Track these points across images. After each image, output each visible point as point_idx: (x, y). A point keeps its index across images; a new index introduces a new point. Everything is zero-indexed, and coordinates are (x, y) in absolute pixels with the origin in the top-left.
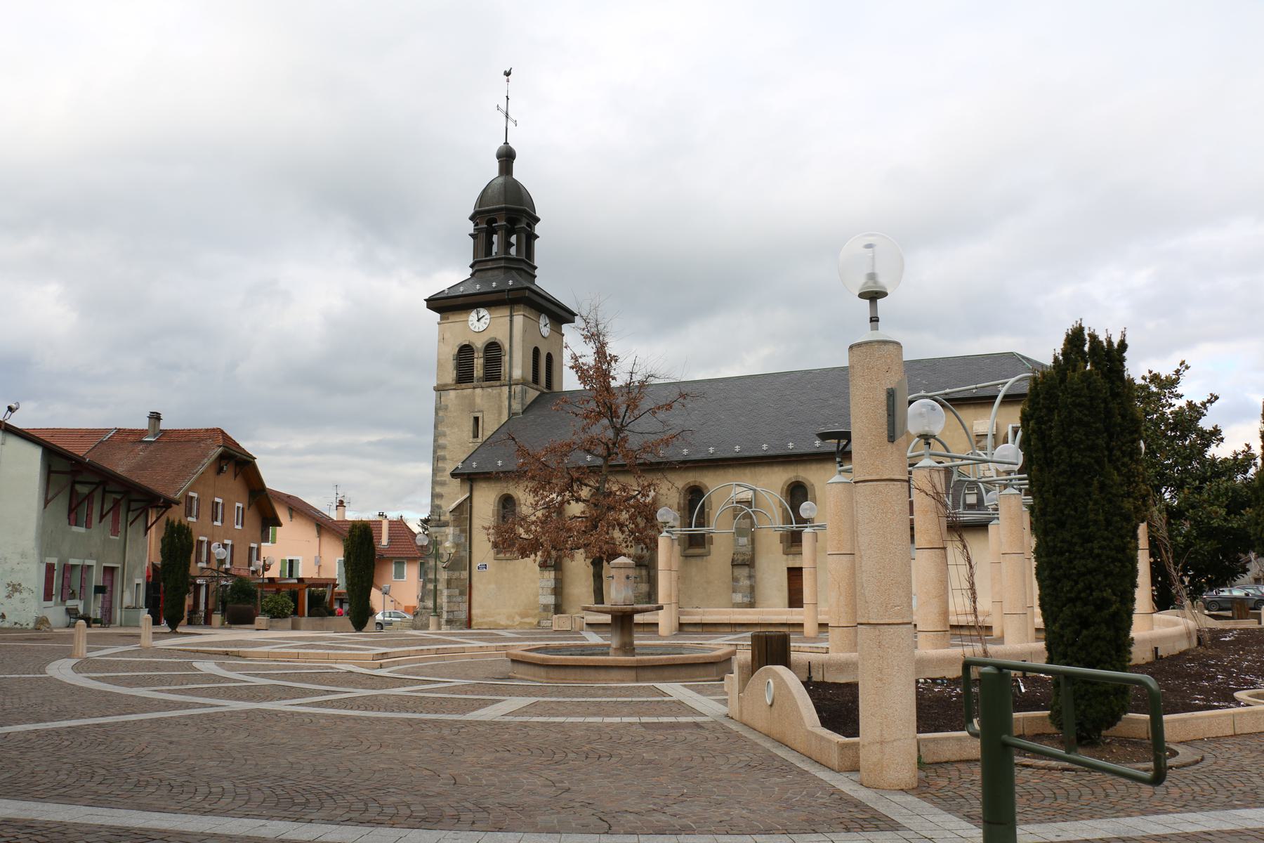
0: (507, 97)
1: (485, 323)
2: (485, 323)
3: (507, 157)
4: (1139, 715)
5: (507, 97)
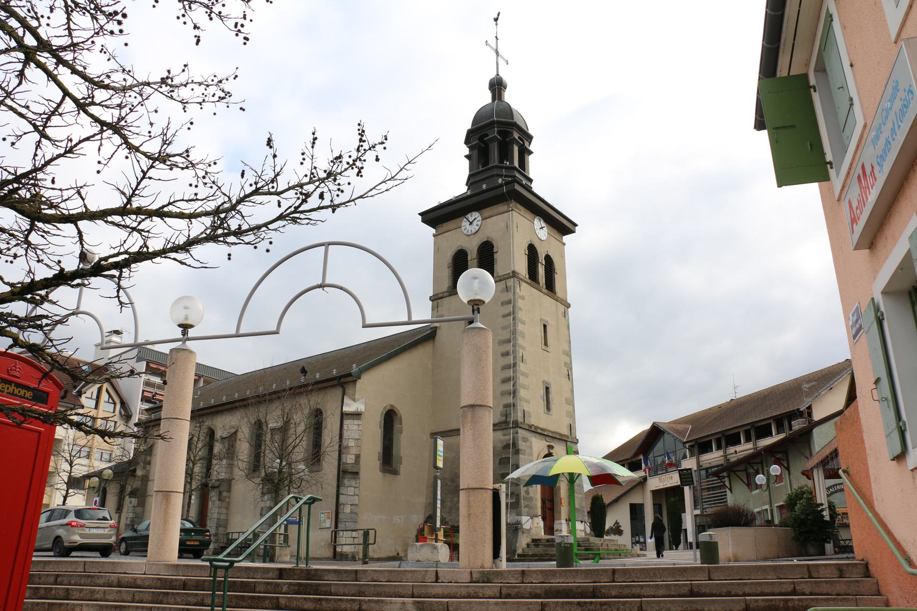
0: (496, 37)
1: (477, 225)
2: (477, 225)
3: (497, 86)
4: (491, 378)
5: (496, 37)
